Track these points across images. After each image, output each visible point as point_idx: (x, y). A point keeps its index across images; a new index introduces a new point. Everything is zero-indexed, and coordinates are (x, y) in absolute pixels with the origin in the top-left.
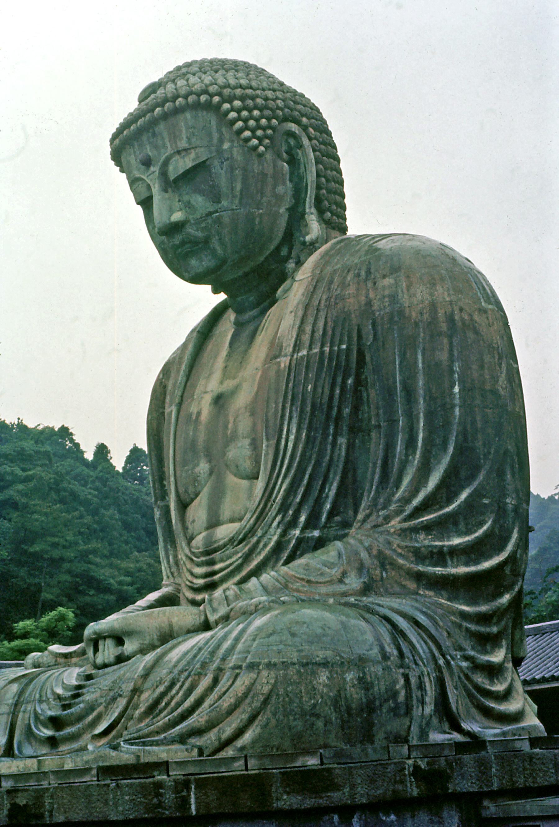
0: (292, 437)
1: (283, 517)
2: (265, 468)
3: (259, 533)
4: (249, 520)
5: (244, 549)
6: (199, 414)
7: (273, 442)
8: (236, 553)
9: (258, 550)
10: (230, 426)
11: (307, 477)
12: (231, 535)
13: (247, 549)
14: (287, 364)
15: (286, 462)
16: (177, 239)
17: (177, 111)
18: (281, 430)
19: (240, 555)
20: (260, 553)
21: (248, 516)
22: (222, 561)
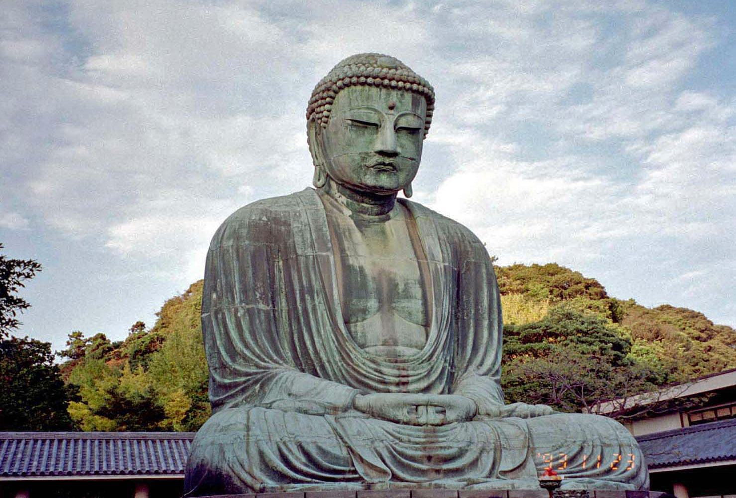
0: (447, 310)
1: (444, 354)
2: (437, 322)
3: (434, 358)
4: (428, 349)
5: (426, 367)
6: (362, 269)
7: (440, 309)
8: (423, 367)
10: (401, 287)
13: (429, 367)
15: (445, 323)
16: (388, 160)
17: (422, 93)
18: (443, 304)
19: (426, 369)
20: (434, 372)
21: (427, 347)
22: (413, 369)
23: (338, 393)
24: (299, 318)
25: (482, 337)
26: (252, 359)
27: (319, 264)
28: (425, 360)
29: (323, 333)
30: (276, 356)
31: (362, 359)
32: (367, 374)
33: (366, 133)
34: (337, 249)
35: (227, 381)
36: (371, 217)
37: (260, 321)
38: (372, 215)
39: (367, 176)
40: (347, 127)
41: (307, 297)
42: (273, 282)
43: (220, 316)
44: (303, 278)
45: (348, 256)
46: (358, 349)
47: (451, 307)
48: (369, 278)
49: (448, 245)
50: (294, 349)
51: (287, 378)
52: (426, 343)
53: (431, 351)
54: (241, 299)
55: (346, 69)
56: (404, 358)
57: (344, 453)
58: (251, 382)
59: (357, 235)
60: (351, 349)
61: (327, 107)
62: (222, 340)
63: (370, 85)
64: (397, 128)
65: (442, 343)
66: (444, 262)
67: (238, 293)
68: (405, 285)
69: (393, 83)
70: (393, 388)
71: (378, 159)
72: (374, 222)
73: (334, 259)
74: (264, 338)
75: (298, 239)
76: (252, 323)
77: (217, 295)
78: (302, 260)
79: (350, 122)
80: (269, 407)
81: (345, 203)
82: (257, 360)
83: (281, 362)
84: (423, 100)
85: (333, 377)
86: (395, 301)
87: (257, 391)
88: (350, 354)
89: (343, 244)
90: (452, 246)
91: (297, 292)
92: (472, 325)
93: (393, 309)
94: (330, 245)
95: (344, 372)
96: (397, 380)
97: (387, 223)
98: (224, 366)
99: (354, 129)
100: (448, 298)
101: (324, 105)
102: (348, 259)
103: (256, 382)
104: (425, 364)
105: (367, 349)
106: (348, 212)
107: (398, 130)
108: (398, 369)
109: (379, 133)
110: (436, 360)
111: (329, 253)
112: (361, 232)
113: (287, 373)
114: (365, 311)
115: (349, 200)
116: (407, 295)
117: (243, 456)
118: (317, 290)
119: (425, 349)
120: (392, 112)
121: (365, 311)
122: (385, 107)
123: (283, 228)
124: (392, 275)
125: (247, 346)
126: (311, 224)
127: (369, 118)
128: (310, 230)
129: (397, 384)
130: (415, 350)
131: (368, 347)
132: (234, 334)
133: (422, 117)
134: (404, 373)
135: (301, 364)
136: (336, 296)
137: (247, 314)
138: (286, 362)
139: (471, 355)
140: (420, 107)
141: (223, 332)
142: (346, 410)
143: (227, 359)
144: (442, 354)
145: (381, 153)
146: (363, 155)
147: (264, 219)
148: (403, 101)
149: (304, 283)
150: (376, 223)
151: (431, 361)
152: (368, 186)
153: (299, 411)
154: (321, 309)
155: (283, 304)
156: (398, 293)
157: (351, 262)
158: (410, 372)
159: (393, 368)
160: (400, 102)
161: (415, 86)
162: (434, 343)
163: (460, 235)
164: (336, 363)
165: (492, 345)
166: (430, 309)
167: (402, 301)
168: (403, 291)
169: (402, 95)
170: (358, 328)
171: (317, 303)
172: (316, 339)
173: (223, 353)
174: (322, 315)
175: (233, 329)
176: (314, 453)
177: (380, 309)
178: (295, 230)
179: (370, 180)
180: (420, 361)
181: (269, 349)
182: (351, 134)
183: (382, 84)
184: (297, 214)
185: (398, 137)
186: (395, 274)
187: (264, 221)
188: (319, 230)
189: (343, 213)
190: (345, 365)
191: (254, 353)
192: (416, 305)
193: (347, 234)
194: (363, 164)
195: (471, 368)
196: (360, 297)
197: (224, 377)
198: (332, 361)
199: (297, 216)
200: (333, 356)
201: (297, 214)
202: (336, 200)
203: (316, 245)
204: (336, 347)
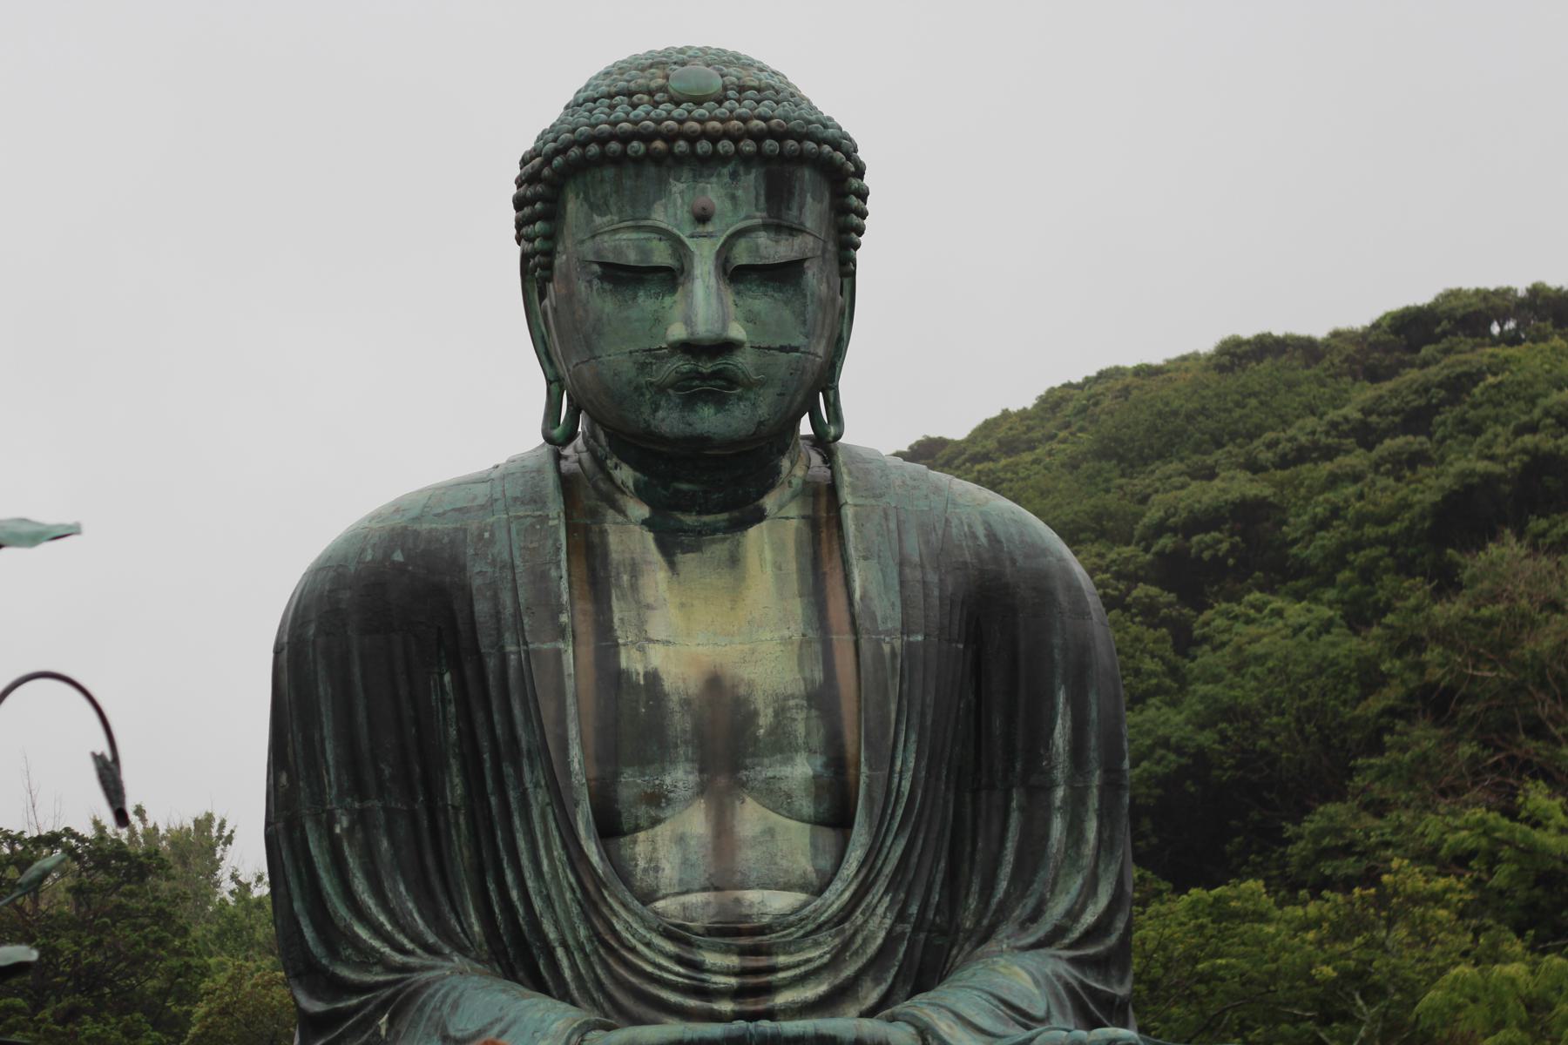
0: (908, 775)
3: (858, 918)
4: (837, 896)
6: (653, 678)
8: (817, 944)
9: (854, 947)
10: (765, 720)
11: (920, 842)
12: (806, 912)
13: (837, 941)
14: (898, 650)
15: (900, 812)
16: (707, 367)
17: (802, 159)
18: (893, 759)
20: (856, 953)
21: (837, 885)
25: (1046, 837)
26: (373, 948)
28: (825, 923)
29: (545, 867)
30: (437, 934)
31: (642, 931)
32: (657, 972)
33: (641, 293)
34: (585, 628)
35: (317, 1007)
36: (706, 518)
37: (392, 843)
38: (709, 513)
39: (660, 414)
40: (590, 282)
41: (508, 770)
43: (297, 834)
44: (496, 717)
45: (617, 645)
46: (636, 905)
47: (924, 763)
48: (674, 704)
49: (933, 578)
51: (446, 995)
52: (835, 874)
53: (847, 895)
54: (340, 786)
56: (766, 920)
58: (371, 1007)
59: (657, 580)
60: (616, 906)
61: (539, 226)
62: (303, 899)
63: (638, 161)
64: (729, 271)
65: (888, 869)
66: (906, 629)
67: (332, 771)
68: (776, 714)
69: (704, 146)
70: (726, 1006)
71: (681, 364)
72: (715, 531)
73: (574, 660)
74: (402, 888)
75: (482, 607)
77: (289, 778)
78: (491, 663)
79: (596, 268)
81: (630, 484)
82: (387, 950)
83: (447, 951)
85: (572, 986)
86: (748, 761)
87: (383, 1032)
88: (614, 921)
89: (610, 608)
90: (950, 580)
91: (486, 756)
92: (1014, 804)
93: (743, 785)
94: (564, 618)
95: (599, 971)
96: (733, 981)
97: (753, 532)
99: (607, 286)
100: (913, 737)
101: (534, 223)
102: (617, 655)
103: (382, 1008)
104: (820, 937)
105: (660, 904)
106: (639, 511)
107: (735, 275)
108: (743, 952)
109: (678, 296)
110: (859, 922)
111: (562, 646)
112: (672, 565)
113: (455, 980)
114: (657, 799)
115: (638, 475)
116: (781, 745)
118: (529, 751)
119: (827, 894)
120: (709, 228)
122: (684, 214)
123: (448, 579)
124: (742, 691)
126: (518, 562)
127: (644, 252)
128: (514, 580)
129: (736, 994)
130: (802, 897)
131: (664, 897)
133: (809, 224)
134: (763, 962)
135: (506, 953)
136: (576, 766)
137: (358, 827)
138: (463, 951)
139: (1007, 893)
140: (797, 198)
141: (305, 877)
143: (317, 950)
144: (887, 899)
145: (689, 348)
146: (642, 359)
147: (398, 557)
148: (739, 193)
149: (499, 731)
150: (720, 535)
151: (847, 925)
152: (662, 439)
154: (539, 799)
155: (455, 788)
156: (756, 740)
157: (624, 664)
158: (782, 960)
159: (727, 950)
160: (733, 198)
161: (770, 145)
162: (858, 871)
163: (983, 540)
164: (582, 949)
165: (1079, 855)
166: (852, 771)
167: (766, 761)
168: (772, 731)
169: (734, 175)
170: (640, 848)
171: (529, 785)
172: (530, 884)
173: (309, 933)
174: (543, 816)
175: (328, 871)
177: (702, 790)
178: (477, 582)
179: (668, 420)
180: (810, 927)
181: (416, 916)
182: (602, 303)
183: (670, 152)
184: (487, 535)
185: (738, 293)
186: (751, 684)
187: (393, 562)
188: (541, 577)
189: (626, 516)
190: (602, 951)
191: (377, 930)
192: (800, 770)
193: (625, 578)
194: (642, 380)
195: (1005, 930)
196: (642, 761)
197: (313, 993)
198: (571, 942)
200: (574, 930)
201: (487, 535)
202: (610, 478)
203: (526, 620)
204: (579, 903)
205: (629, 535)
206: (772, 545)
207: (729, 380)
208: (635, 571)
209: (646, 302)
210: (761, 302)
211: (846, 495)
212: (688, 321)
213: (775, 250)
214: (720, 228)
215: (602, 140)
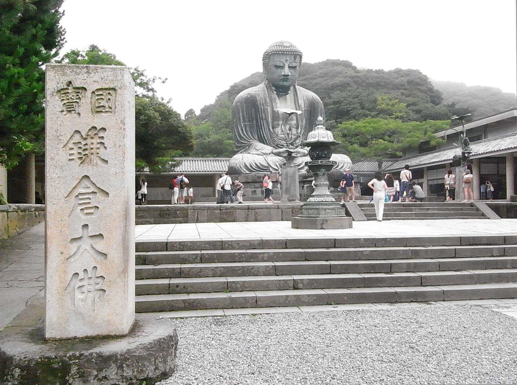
23: (268, 149)
24: (259, 128)
27: (265, 111)
34: (270, 106)
42: (252, 115)
50: (258, 136)
55: (273, 48)
57: (267, 165)
76: (246, 129)
80: (249, 153)
84: (298, 57)
98: (238, 140)
106: (276, 93)
107: (289, 67)
114: (278, 125)
117: (242, 166)
121: (278, 125)
125: (244, 135)
132: (240, 132)
142: (270, 154)
145: (284, 75)
153: (256, 154)
176: (259, 165)
179: (281, 83)
182: (274, 69)
196: (277, 121)
199: (259, 95)
205: (275, 95)
206: (290, 96)
207: (288, 79)
208: (275, 99)
209: (279, 70)
210: (292, 71)
211: (298, 92)
212: (284, 72)
213: (294, 65)
214: (288, 62)
215: (276, 51)
